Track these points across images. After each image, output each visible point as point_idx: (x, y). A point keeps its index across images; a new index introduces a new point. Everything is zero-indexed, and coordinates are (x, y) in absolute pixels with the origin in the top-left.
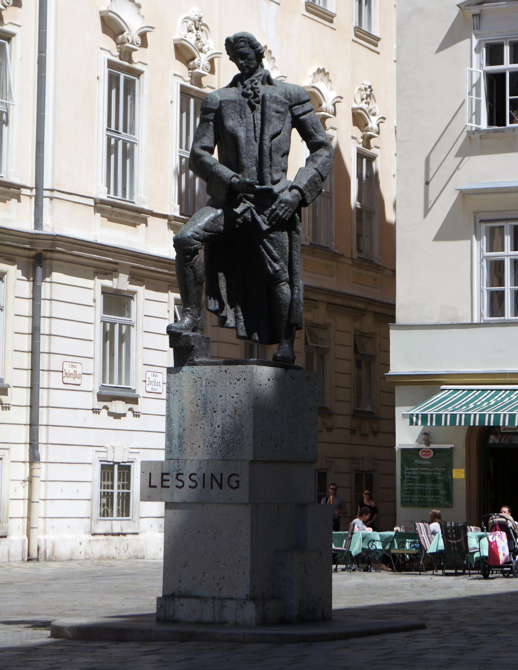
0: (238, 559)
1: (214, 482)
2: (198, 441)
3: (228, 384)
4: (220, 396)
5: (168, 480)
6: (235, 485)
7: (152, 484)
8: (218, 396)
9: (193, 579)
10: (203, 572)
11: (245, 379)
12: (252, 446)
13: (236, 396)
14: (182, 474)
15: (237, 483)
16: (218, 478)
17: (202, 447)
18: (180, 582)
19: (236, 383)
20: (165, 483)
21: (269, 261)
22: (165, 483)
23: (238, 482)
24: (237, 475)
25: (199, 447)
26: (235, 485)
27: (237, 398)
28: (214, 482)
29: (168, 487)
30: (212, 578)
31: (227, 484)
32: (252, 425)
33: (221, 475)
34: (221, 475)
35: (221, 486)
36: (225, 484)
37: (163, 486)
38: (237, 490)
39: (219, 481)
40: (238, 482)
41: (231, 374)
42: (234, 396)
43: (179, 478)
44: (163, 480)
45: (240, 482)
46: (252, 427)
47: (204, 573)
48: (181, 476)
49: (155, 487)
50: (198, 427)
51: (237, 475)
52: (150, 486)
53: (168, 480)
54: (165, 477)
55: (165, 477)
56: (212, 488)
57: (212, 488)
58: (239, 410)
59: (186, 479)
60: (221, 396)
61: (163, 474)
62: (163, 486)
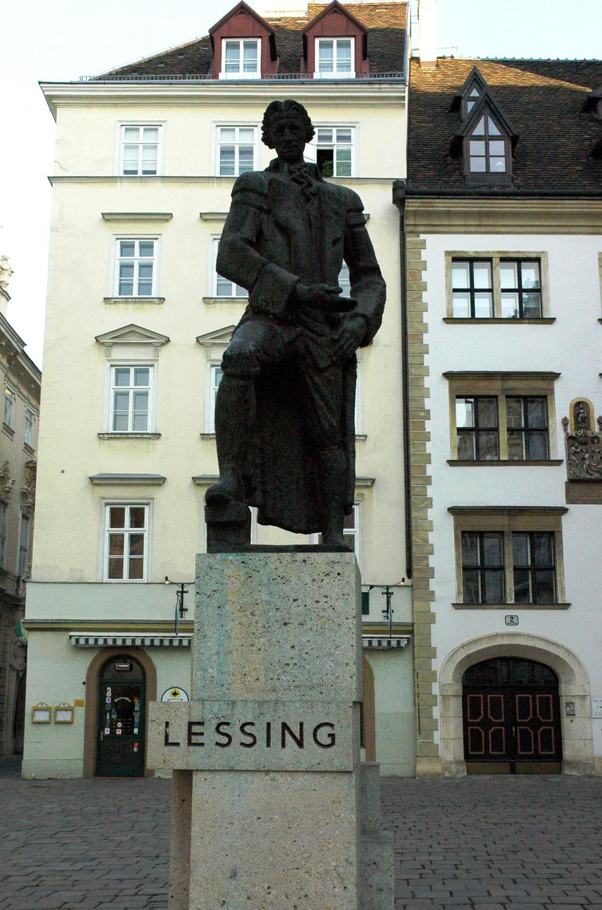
0: (334, 864)
1: (288, 737)
2: (255, 669)
3: (308, 580)
4: (295, 600)
5: (202, 734)
6: (328, 741)
7: (171, 740)
8: (291, 600)
9: (249, 898)
10: (266, 887)
11: (339, 574)
12: (355, 678)
13: (325, 600)
14: (228, 724)
15: (330, 738)
16: (296, 730)
17: (262, 679)
18: (222, 905)
19: (322, 580)
20: (195, 739)
21: (324, 413)
22: (195, 739)
23: (332, 736)
24: (332, 725)
25: (258, 679)
26: (328, 741)
27: (326, 602)
28: (288, 737)
29: (202, 744)
30: (284, 897)
31: (312, 740)
32: (355, 645)
33: (301, 724)
34: (301, 724)
35: (300, 743)
36: (308, 738)
37: (190, 744)
38: (331, 749)
39: (298, 735)
40: (332, 736)
41: (313, 565)
42: (320, 600)
43: (221, 731)
44: (190, 734)
45: (336, 737)
46: (355, 648)
47: (269, 888)
48: (225, 727)
49: (177, 744)
50: (254, 648)
51: (332, 725)
52: (167, 743)
53: (202, 734)
54: (195, 729)
55: (195, 729)
56: (283, 745)
57: (283, 745)
58: (330, 621)
59: (234, 731)
60: (297, 600)
61: (191, 724)
62: (190, 744)
